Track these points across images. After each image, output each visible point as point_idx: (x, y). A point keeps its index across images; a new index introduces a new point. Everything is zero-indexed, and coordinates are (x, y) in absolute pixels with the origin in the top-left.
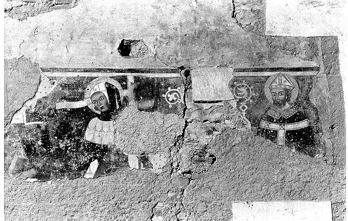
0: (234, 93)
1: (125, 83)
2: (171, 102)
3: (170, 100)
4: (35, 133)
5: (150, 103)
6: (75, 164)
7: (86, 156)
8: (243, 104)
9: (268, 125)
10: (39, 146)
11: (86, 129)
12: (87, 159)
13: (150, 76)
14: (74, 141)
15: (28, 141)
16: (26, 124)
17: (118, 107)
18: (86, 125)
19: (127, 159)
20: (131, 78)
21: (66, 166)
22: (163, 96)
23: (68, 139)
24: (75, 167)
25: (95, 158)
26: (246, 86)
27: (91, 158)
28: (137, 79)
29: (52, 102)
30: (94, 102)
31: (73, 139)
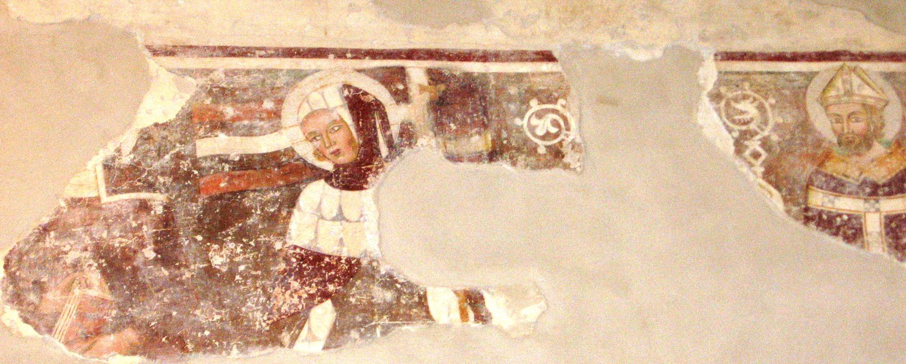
0: (723, 114)
1: (401, 87)
2: (543, 138)
3: (540, 132)
4: (134, 224)
5: (479, 142)
6: (263, 312)
7: (296, 291)
8: (754, 145)
9: (833, 202)
10: (146, 262)
11: (290, 213)
12: (300, 297)
13: (475, 67)
14: (257, 248)
15: (110, 249)
16: (105, 199)
17: (384, 150)
18: (292, 201)
19: (423, 299)
20: (417, 72)
21: (236, 319)
22: (518, 122)
23: (237, 240)
24: (260, 321)
25: (326, 295)
26: (755, 99)
27: (311, 297)
28: (435, 77)
29: (184, 136)
30: (312, 137)
31: (252, 243)
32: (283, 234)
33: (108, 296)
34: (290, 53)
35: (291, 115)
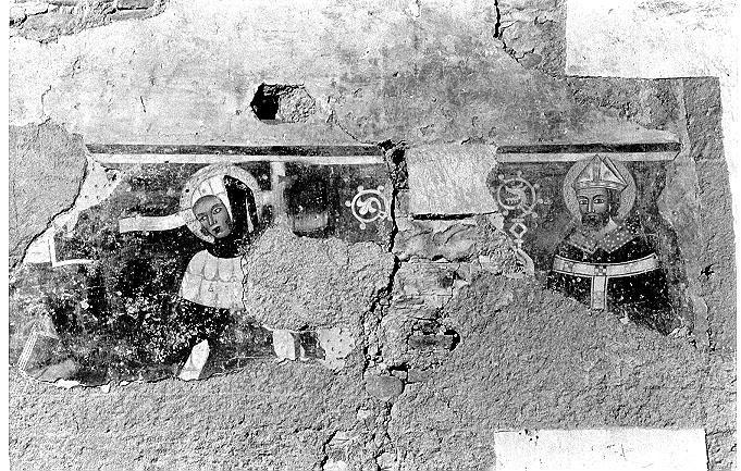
0: (499, 197)
1: (265, 178)
2: (365, 217)
3: (363, 212)
4: (75, 283)
5: (319, 221)
6: (160, 349)
7: (183, 333)
8: (518, 222)
9: (571, 267)
10: (83, 312)
11: (182, 275)
12: (186, 338)
13: (320, 161)
14: (159, 301)
15: (59, 301)
16: (55, 264)
17: (251, 228)
18: (183, 266)
19: (270, 339)
20: (278, 165)
21: (141, 353)
22: (348, 204)
23: (144, 296)
24: (159, 355)
25: (203, 336)
26: (524, 184)
27: (194, 338)
28: (291, 169)
29: (111, 216)
30: (201, 217)
31: (155, 297)
33: (55, 336)
34: (183, 151)
35: (185, 203)
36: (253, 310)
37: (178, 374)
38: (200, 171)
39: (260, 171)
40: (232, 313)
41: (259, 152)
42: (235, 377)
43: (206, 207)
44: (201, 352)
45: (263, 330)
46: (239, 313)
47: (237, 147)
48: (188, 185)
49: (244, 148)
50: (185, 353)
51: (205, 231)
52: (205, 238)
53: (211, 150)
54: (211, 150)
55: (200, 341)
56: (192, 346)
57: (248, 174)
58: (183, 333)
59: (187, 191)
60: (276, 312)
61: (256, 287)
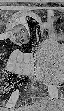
1: (45, 17)
7: (8, 87)
11: (7, 60)
17: (38, 39)
19: (47, 90)
20: (50, 11)
25: (17, 88)
27: (13, 89)
28: (57, 13)
30: (15, 35)
32: (4, 67)
35: (9, 28)
36: (40, 76)
37: (5, 105)
38: (15, 14)
39: (43, 14)
40: (29, 78)
41: (42, 6)
42: (31, 106)
43: (18, 30)
44: (16, 95)
45: (44, 85)
46: (33, 78)
47: (32, 3)
48: (10, 20)
49: (35, 4)
50: (8, 96)
51: (17, 41)
52: (18, 44)
53: (20, 4)
54: (20, 4)
55: (15, 90)
56: (11, 93)
57: (37, 15)
58: (8, 87)
59: (9, 23)
60: (50, 77)
61: (41, 66)
